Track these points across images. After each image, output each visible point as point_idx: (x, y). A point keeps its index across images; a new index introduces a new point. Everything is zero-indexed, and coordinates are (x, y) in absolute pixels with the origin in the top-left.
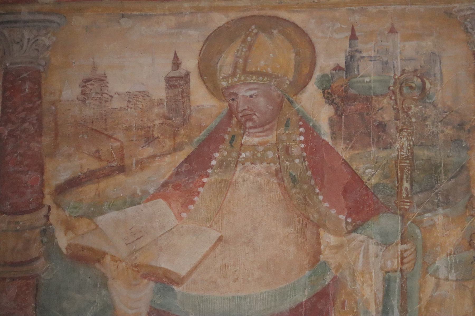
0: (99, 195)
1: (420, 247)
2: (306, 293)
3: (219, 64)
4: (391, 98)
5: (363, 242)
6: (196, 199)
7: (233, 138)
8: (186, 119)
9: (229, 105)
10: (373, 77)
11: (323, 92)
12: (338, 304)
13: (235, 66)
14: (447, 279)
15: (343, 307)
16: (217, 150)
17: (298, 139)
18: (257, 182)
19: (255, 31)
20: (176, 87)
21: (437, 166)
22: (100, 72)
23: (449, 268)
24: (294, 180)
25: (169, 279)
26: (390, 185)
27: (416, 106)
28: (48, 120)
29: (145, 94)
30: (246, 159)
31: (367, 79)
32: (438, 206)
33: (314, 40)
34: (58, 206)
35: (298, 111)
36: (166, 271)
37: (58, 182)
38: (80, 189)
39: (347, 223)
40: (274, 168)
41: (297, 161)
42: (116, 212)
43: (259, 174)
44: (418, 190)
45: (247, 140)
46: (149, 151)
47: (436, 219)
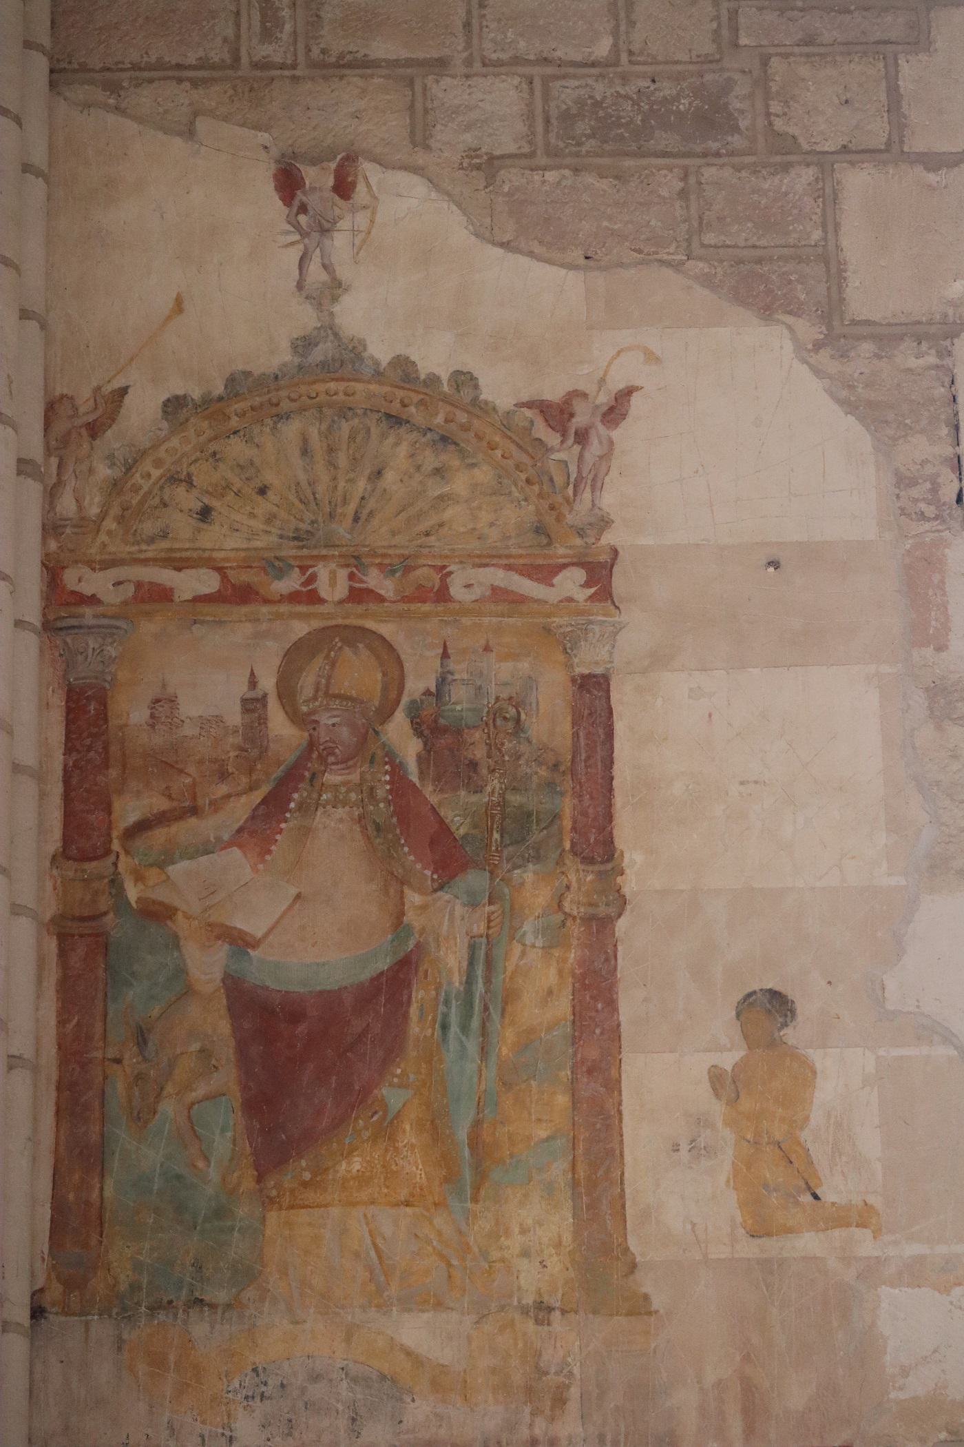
0: (170, 840)
1: (508, 906)
2: (388, 961)
3: (299, 685)
4: (484, 730)
5: (449, 902)
6: (273, 848)
7: (313, 776)
8: (264, 750)
9: (310, 735)
10: (465, 705)
11: (412, 722)
12: (421, 974)
13: (317, 690)
14: (533, 946)
15: (426, 977)
16: (296, 790)
17: (383, 779)
18: (338, 829)
19: (339, 644)
20: (252, 711)
21: (529, 815)
22: (170, 690)
23: (536, 933)
24: (378, 828)
25: (243, 940)
26: (479, 837)
27: (510, 741)
28: (114, 749)
29: (219, 719)
30: (327, 802)
31: (458, 708)
32: (529, 861)
33: (403, 657)
34: (127, 852)
35: (384, 745)
36: (240, 931)
37: (126, 825)
38: (150, 833)
39: (433, 880)
40: (357, 814)
41: (382, 805)
42: (188, 862)
43: (341, 820)
44: (508, 842)
45: (331, 778)
46: (223, 789)
47: (525, 876)
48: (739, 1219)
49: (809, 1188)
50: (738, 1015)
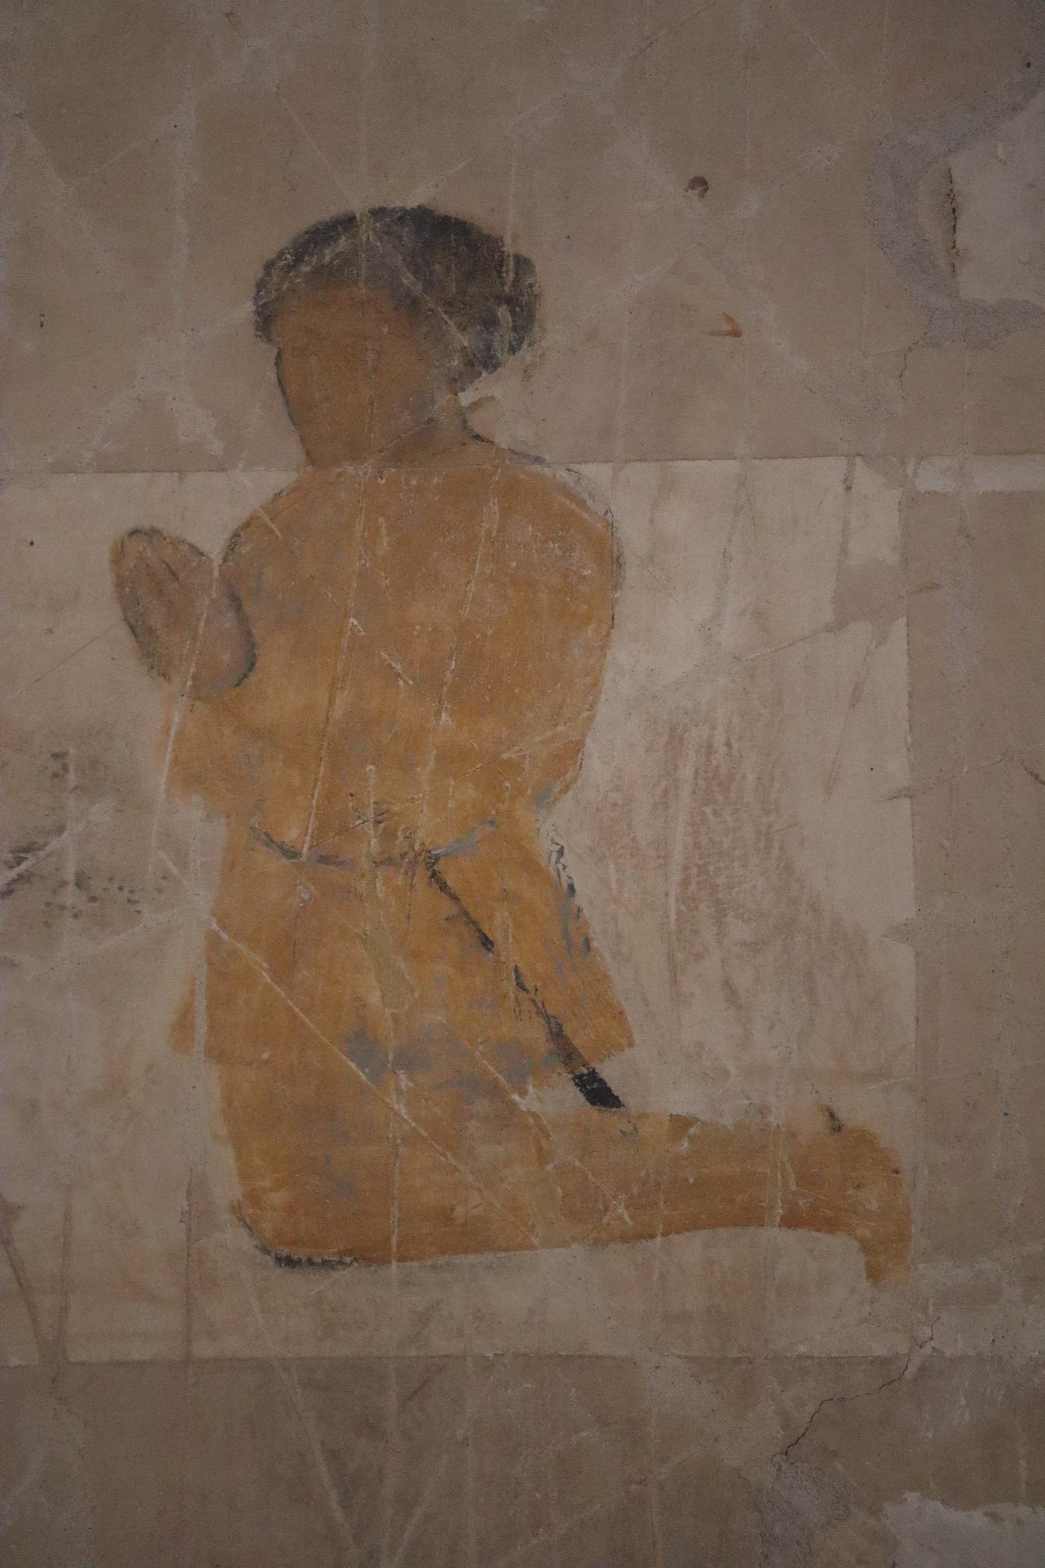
48: (227, 1189)
49: (567, 1054)
50: (266, 321)
